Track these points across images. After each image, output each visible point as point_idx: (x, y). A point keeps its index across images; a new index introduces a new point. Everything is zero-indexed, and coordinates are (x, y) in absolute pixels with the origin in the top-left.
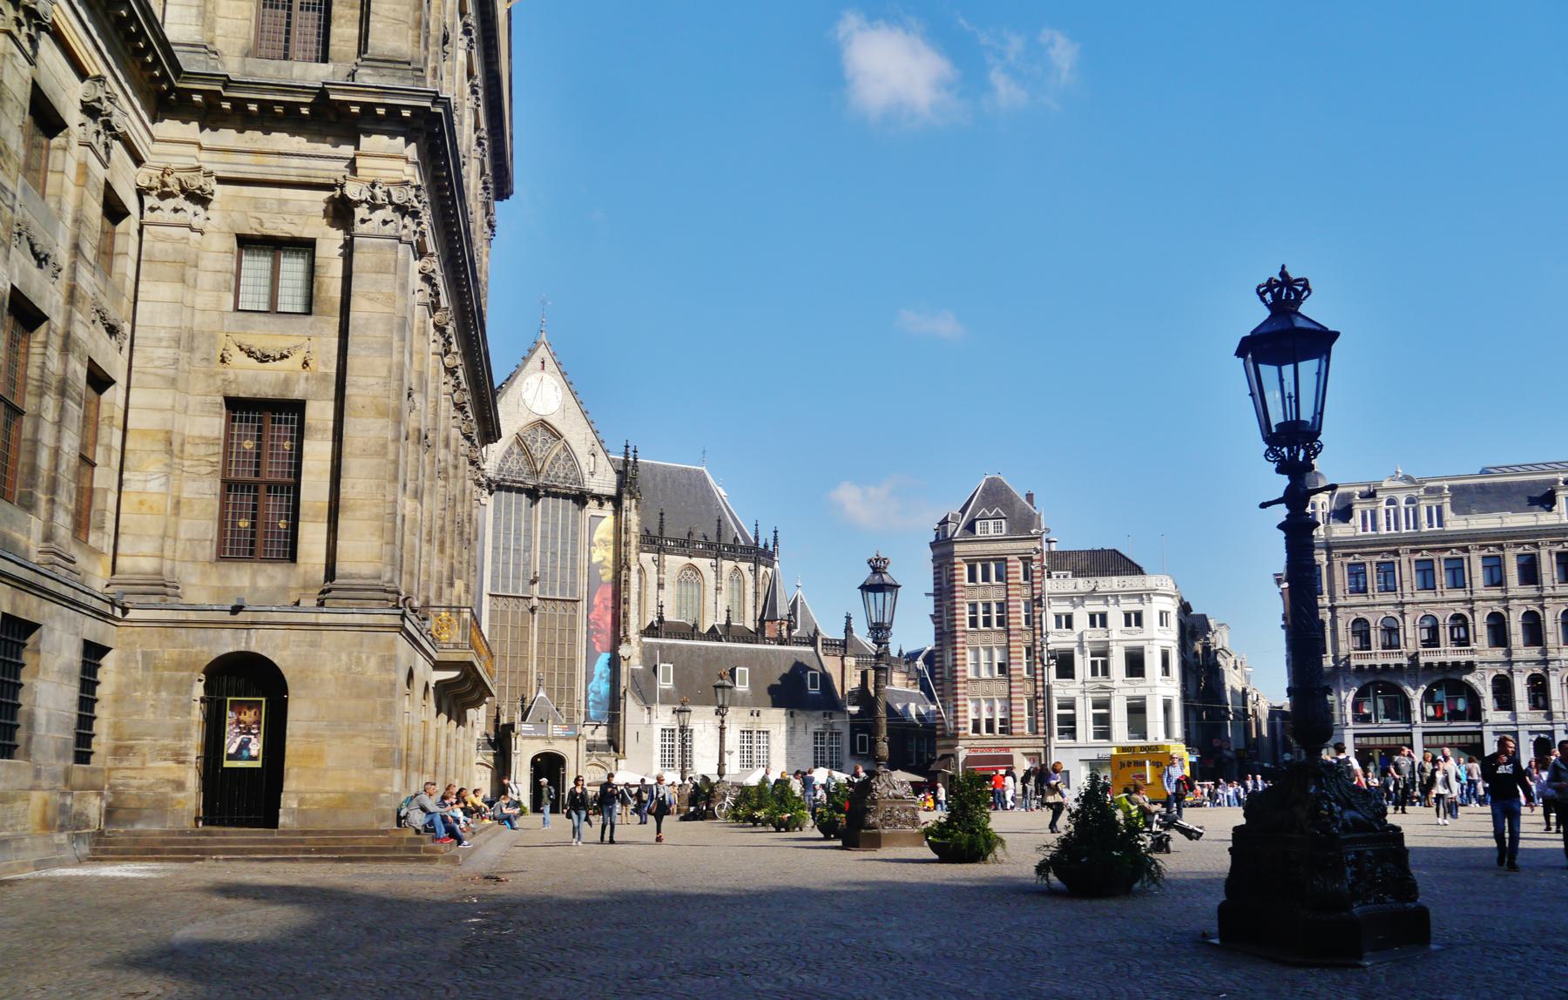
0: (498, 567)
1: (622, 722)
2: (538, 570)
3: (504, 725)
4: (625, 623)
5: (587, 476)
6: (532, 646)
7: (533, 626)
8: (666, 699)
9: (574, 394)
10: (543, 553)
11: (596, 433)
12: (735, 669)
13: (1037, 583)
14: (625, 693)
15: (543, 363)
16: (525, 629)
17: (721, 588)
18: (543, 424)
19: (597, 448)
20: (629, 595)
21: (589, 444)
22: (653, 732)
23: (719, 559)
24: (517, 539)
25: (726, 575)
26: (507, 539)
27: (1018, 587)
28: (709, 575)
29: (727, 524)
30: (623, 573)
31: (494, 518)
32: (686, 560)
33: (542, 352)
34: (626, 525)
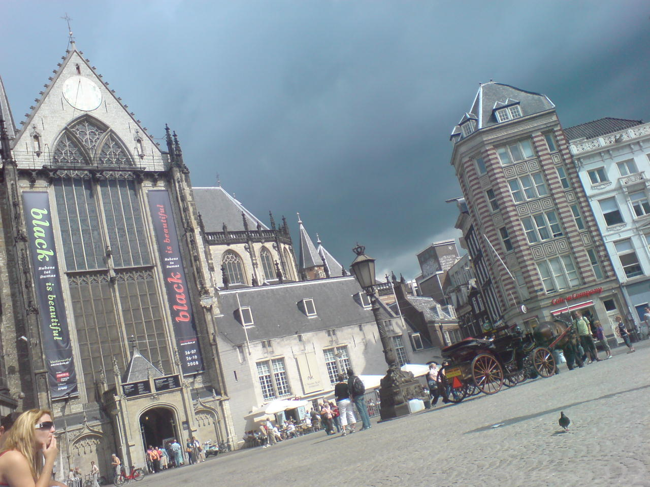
0: (71, 248)
1: (217, 366)
2: (109, 244)
3: (106, 393)
4: (199, 277)
5: (136, 158)
6: (118, 315)
7: (115, 296)
8: (254, 336)
9: (112, 92)
10: (111, 230)
11: (138, 122)
12: (302, 301)
13: (564, 149)
14: (214, 340)
15: (78, 68)
16: (108, 299)
17: (257, 263)
18: (87, 119)
19: (141, 134)
20: (198, 252)
21: (133, 132)
22: (249, 366)
23: (250, 242)
24: (84, 221)
25: (257, 254)
26: (74, 221)
27: (549, 156)
28: (245, 256)
29: (248, 219)
30: (188, 234)
31: (58, 204)
32: (225, 248)
33: (75, 59)
34: (181, 193)
